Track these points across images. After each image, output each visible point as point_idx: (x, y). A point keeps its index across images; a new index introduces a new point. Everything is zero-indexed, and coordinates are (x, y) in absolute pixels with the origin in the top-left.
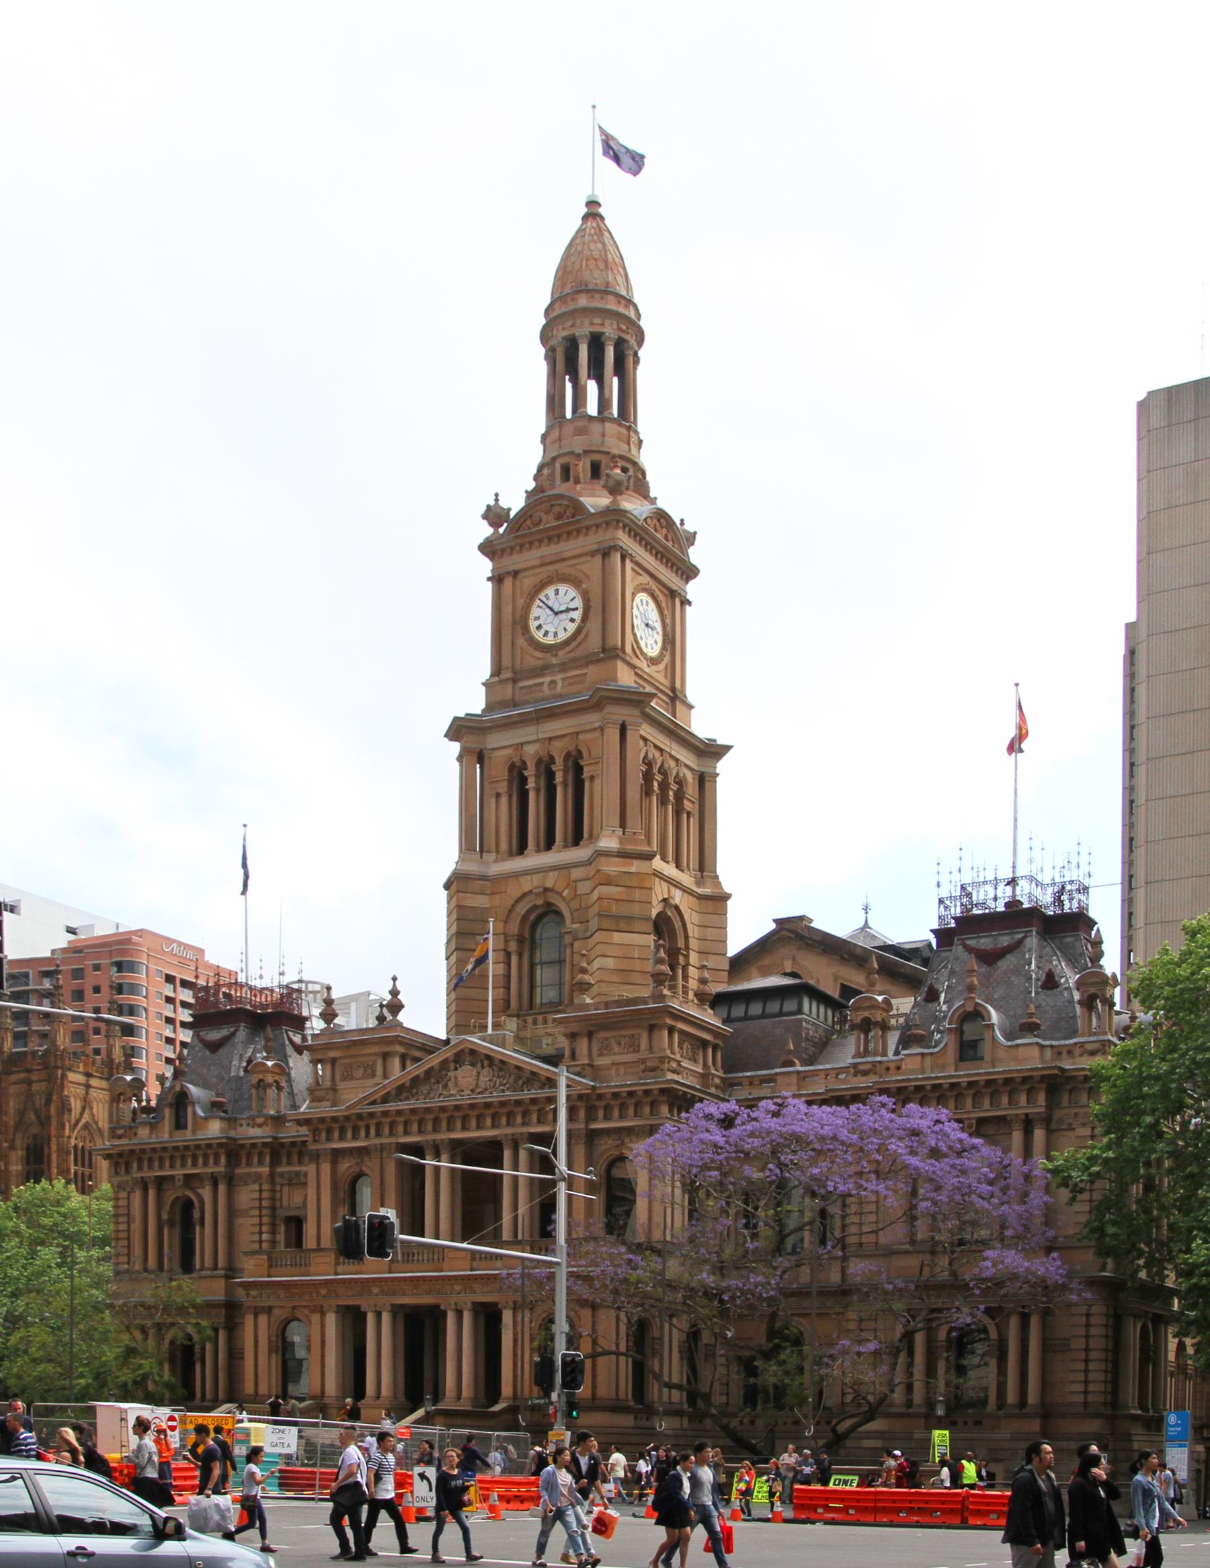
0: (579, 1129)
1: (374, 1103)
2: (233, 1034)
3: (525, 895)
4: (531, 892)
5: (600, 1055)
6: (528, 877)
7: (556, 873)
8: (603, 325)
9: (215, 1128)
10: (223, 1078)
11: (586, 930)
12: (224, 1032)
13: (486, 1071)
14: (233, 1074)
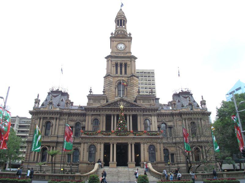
1: (103, 106)
2: (58, 95)
9: (58, 109)
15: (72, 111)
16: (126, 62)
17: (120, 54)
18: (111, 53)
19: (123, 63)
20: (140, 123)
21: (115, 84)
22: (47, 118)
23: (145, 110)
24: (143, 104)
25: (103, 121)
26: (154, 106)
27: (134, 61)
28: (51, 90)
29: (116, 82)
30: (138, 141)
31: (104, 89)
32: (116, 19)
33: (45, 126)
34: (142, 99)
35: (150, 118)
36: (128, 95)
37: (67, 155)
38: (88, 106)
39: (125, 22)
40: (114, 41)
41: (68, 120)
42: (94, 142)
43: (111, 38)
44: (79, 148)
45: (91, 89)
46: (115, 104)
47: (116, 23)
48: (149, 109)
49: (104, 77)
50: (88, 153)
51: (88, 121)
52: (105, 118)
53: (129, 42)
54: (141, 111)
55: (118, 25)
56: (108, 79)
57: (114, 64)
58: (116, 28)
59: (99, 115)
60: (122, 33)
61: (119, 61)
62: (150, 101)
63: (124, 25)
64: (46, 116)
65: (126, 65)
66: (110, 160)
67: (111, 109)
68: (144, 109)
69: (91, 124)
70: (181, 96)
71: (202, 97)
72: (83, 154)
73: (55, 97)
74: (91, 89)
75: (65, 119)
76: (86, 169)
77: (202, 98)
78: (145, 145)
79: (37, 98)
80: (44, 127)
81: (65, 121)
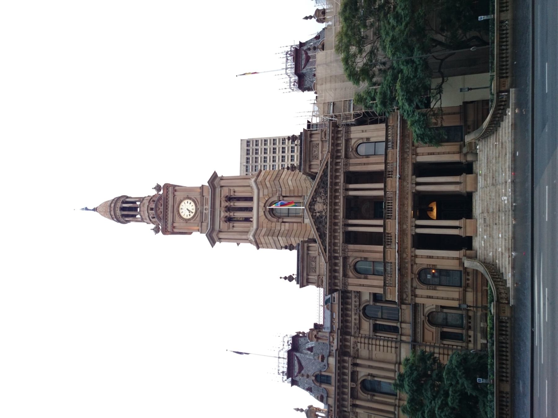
0: (344, 162)
1: (325, 250)
2: (297, 357)
3: (265, 214)
4: (264, 212)
5: (318, 159)
6: (259, 213)
7: (260, 202)
8: (118, 207)
10: (314, 363)
11: (279, 190)
12: (296, 363)
13: (318, 199)
14: (312, 358)
15: (336, 326)
16: (223, 199)
17: (204, 211)
18: (201, 233)
19: (224, 204)
20: (364, 164)
21: (274, 224)
22: (352, 388)
23: (334, 154)
24: (320, 158)
25: (360, 251)
26: (325, 134)
27: (222, 178)
28: (285, 377)
29: (269, 220)
30: (409, 169)
31: (286, 248)
32: (118, 221)
33: (374, 395)
34: (310, 161)
35: (353, 142)
36: (300, 194)
37: (445, 342)
38: (324, 283)
39: (128, 200)
40: (172, 224)
41: (357, 335)
42: (412, 273)
43: (165, 232)
44: (426, 310)
45: (285, 278)
46: (320, 223)
47: (129, 221)
48: (333, 144)
49: (258, 248)
50: (439, 288)
51: (360, 285)
52: (351, 247)
53: (175, 191)
54: (337, 164)
55: (134, 216)
56: (262, 240)
57: (226, 224)
58: (142, 220)
59: (345, 259)
60: (153, 206)
61: (221, 214)
62: (314, 142)
63: (134, 203)
64: (348, 391)
65: (229, 199)
66: (458, 235)
67: (333, 231)
68: (332, 157)
69: (366, 278)
70: (304, 71)
71: (306, 18)
72: (443, 298)
73: (301, 367)
74: (285, 278)
75: (356, 343)
76: (479, 294)
77: (311, 17)
78: (419, 150)
79: (304, 413)
80: (376, 398)
81: (359, 344)
